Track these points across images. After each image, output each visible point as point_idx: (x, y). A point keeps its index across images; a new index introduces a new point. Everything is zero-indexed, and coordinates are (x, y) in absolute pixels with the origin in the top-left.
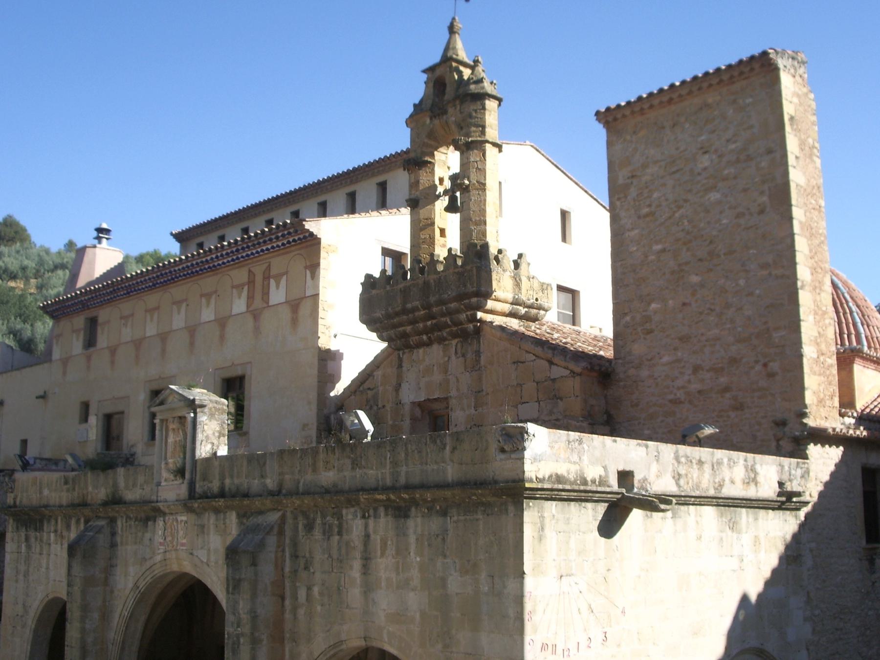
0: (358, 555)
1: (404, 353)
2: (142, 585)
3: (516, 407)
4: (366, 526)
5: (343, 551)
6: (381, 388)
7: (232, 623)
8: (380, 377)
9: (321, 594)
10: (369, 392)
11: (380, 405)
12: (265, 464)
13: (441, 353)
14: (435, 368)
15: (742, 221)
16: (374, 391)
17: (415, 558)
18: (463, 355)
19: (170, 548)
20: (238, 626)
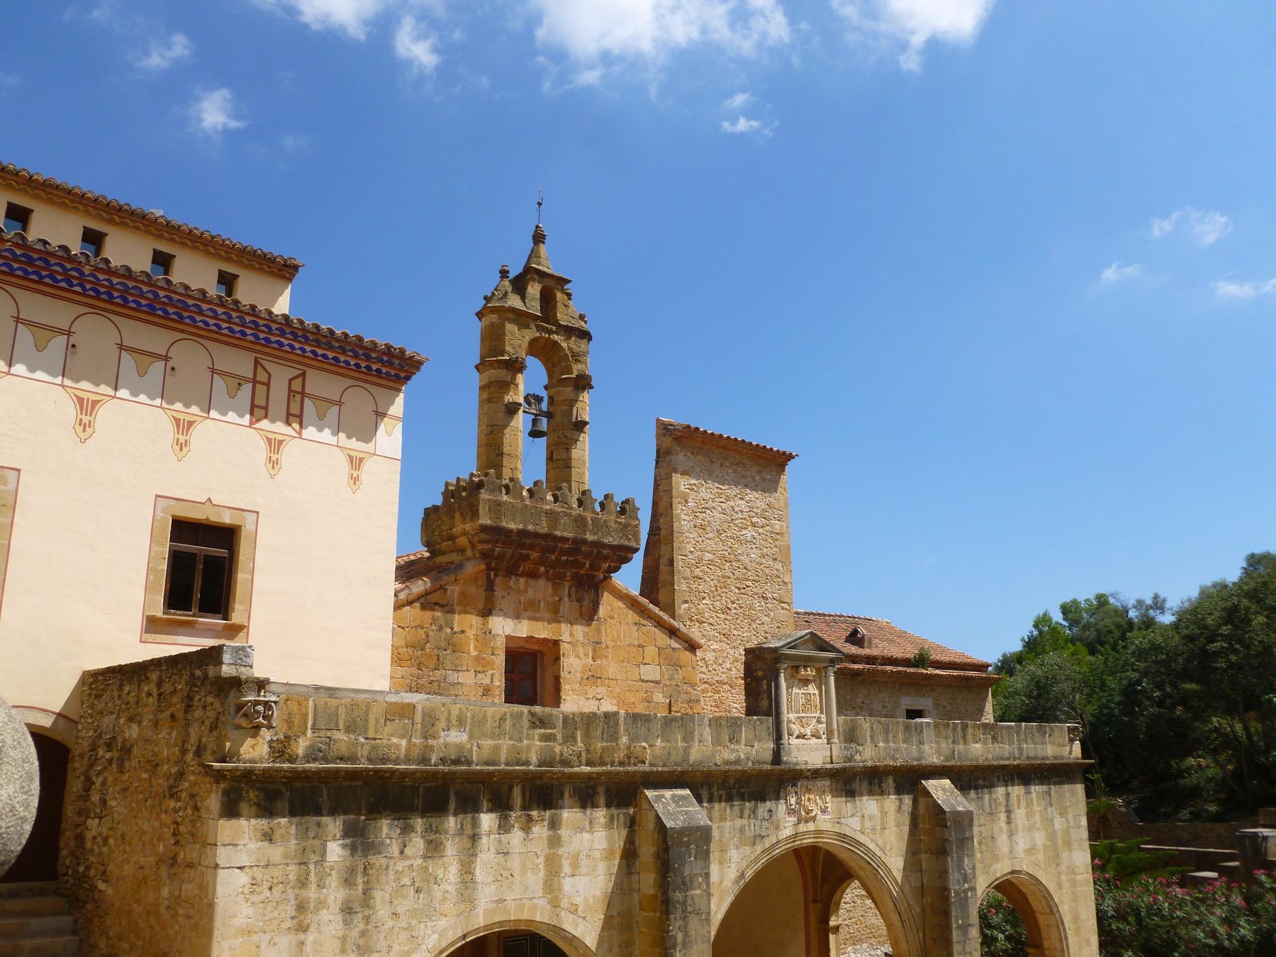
1: (496, 575)
2: (749, 874)
3: (638, 666)
5: (993, 807)
7: (958, 881)
8: (456, 594)
12: (922, 731)
13: (550, 591)
14: (542, 604)
15: (763, 560)
17: (1036, 808)
18: (579, 601)
20: (965, 881)
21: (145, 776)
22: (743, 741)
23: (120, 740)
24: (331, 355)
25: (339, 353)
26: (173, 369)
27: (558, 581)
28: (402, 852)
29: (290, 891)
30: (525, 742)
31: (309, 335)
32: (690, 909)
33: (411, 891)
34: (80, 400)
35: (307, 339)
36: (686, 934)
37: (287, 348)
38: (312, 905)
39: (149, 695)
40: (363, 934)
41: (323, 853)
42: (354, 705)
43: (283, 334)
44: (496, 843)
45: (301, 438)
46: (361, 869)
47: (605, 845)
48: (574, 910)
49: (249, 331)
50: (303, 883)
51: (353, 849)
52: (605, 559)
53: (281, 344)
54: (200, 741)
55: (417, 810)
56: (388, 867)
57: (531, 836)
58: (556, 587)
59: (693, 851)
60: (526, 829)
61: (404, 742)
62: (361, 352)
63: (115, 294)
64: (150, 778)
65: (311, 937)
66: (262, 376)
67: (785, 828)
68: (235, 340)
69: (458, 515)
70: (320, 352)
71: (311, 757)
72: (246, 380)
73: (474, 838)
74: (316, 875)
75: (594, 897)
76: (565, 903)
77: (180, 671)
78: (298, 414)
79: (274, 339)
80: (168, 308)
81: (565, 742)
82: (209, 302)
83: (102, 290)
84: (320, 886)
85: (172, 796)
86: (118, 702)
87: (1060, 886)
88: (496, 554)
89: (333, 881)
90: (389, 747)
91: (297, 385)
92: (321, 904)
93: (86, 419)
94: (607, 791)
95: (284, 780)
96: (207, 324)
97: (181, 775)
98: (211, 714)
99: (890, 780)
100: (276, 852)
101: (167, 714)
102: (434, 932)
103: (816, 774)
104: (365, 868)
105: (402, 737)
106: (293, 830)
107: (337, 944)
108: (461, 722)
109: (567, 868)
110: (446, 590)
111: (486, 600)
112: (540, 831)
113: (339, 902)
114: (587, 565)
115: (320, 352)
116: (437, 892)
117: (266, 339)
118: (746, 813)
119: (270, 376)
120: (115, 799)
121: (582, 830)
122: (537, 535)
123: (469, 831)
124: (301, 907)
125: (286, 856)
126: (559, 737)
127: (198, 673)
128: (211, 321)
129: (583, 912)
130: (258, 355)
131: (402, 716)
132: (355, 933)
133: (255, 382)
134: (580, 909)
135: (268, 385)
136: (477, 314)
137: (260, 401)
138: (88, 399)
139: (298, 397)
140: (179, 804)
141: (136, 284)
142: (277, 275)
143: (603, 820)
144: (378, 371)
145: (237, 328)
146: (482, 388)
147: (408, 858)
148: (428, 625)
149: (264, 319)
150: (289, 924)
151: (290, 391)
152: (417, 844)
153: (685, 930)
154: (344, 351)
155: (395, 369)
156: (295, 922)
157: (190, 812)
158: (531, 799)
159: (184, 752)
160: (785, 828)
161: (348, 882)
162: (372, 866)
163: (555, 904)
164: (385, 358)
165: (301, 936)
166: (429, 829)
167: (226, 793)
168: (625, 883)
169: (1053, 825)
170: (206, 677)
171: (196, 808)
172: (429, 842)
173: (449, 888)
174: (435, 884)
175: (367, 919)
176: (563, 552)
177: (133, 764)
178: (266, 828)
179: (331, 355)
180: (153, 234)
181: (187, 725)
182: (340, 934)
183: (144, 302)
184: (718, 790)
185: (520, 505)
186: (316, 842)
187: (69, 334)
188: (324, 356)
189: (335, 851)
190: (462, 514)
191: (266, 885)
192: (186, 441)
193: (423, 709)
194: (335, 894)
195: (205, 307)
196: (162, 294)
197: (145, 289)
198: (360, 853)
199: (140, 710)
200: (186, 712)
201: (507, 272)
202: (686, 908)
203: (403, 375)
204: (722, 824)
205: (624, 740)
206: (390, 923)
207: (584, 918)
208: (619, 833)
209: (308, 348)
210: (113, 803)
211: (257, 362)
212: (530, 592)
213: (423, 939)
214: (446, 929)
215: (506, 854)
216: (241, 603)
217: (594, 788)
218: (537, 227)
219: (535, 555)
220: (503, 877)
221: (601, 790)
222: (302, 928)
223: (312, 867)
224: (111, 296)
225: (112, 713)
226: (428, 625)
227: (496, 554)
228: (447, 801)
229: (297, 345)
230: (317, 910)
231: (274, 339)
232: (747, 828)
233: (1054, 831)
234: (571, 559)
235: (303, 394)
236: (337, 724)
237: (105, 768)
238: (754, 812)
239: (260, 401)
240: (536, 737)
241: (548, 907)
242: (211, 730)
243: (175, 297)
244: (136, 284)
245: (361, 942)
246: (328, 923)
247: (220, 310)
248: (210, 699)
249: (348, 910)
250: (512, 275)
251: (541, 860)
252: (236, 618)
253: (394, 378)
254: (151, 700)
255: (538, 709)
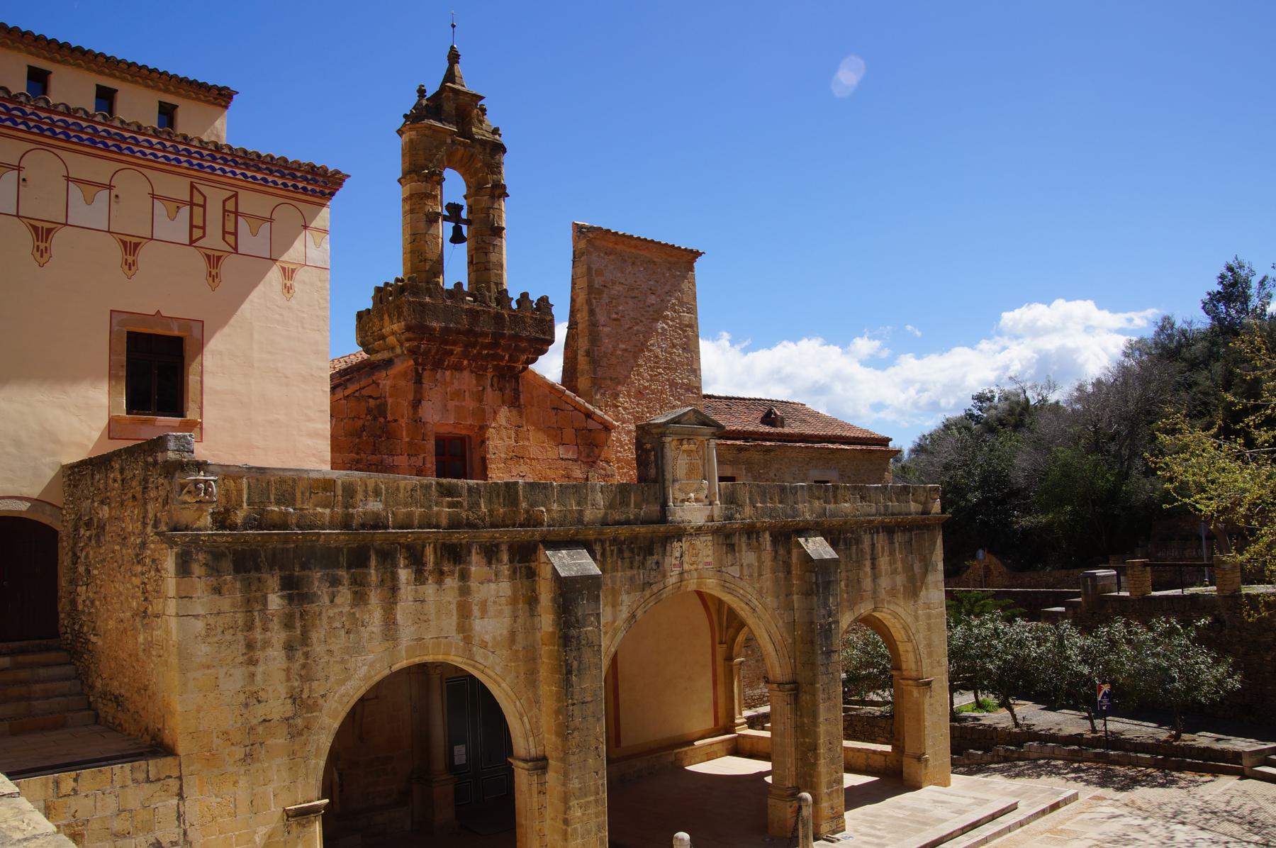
0: (868, 557)
1: (424, 370)
4: (872, 539)
5: (860, 556)
6: (390, 401)
7: (824, 616)
8: (388, 388)
9: (847, 586)
10: (370, 400)
11: (390, 418)
12: (796, 493)
13: (474, 382)
14: (467, 394)
16: (379, 401)
17: (898, 556)
18: (500, 390)
19: (686, 567)
20: (829, 617)
21: (117, 547)
22: (632, 505)
23: (95, 520)
24: (259, 176)
25: (266, 174)
26: (117, 196)
27: (481, 373)
28: (332, 601)
29: (239, 634)
30: (435, 509)
31: (237, 159)
32: (583, 642)
33: (343, 632)
34: (35, 229)
35: (236, 163)
36: (580, 663)
37: (219, 172)
38: (259, 645)
39: (115, 481)
40: (304, 666)
41: (265, 604)
42: (283, 481)
43: (214, 159)
44: (413, 593)
45: (237, 253)
46: (298, 615)
47: (509, 593)
48: (484, 645)
49: (183, 159)
50: (249, 627)
51: (290, 599)
52: (524, 351)
53: (213, 169)
54: (156, 515)
55: (343, 567)
56: (320, 613)
57: (444, 587)
58: (480, 378)
59: (586, 596)
60: (440, 582)
61: (328, 511)
62: (286, 172)
63: (58, 131)
64: (121, 549)
65: (260, 670)
66: (198, 199)
67: (671, 576)
68: (172, 165)
69: (386, 317)
70: (249, 174)
71: (248, 524)
72: (183, 202)
73: (394, 589)
74: (261, 620)
75: (501, 635)
76: (476, 641)
77: (136, 459)
78: (233, 231)
79: (206, 164)
80: (107, 141)
81: (470, 508)
82: (144, 134)
83: (45, 127)
84: (265, 629)
85: (139, 562)
86: (92, 489)
87: (917, 618)
88: (422, 350)
89: (275, 625)
90: (315, 515)
91: (230, 206)
92: (266, 644)
93: (42, 246)
94: (511, 548)
95: (227, 545)
96: (144, 154)
97: (144, 545)
98: (163, 493)
99: (767, 535)
100: (225, 603)
101: (130, 495)
102: (364, 665)
103: (699, 531)
104: (302, 615)
105: (325, 507)
106: (238, 585)
107: (283, 674)
108: (377, 493)
109: (476, 611)
110: (378, 385)
111: (415, 392)
112: (451, 583)
113: (282, 642)
114: (507, 358)
115: (249, 174)
116: (365, 633)
117: (200, 165)
118: (636, 564)
119: (205, 198)
120: (96, 568)
121: (490, 581)
122: (458, 332)
123: (389, 584)
124: (250, 646)
125: (233, 605)
126: (465, 504)
127: (150, 459)
128: (148, 151)
129: (492, 647)
130: (193, 180)
131: (325, 489)
132: (297, 666)
133: (192, 204)
134: (490, 644)
135: (204, 206)
136: (398, 132)
137: (198, 221)
138: (42, 228)
139: (233, 216)
140: (144, 568)
141: (75, 121)
142: (213, 104)
143: (507, 573)
144: (304, 189)
145: (172, 157)
146: (404, 200)
147: (336, 606)
148: (364, 416)
149: (195, 146)
150: (241, 659)
151: (225, 211)
152: (345, 595)
153: (579, 659)
154: (271, 173)
155: (319, 186)
156: (246, 657)
157: (153, 573)
158: (442, 555)
159: (145, 525)
160: (671, 576)
161: (288, 624)
162: (307, 612)
163: (468, 640)
164: (309, 177)
165: (252, 668)
166: (353, 582)
167: (178, 556)
168: (528, 623)
169: (913, 569)
170: (156, 463)
171: (158, 570)
172: (355, 593)
173: (375, 630)
174: (363, 626)
175: (306, 655)
176: (484, 347)
177: (107, 539)
178: (215, 583)
179: (259, 176)
180: (95, 71)
181: (146, 503)
182: (285, 666)
183: (85, 137)
184: (610, 546)
185: (442, 306)
186: (259, 594)
187: (19, 168)
188: (254, 178)
189: (275, 602)
190: (389, 316)
191: (220, 630)
192: (134, 261)
193: (343, 483)
194: (278, 636)
195: (140, 138)
196: (100, 128)
197: (84, 124)
198: (296, 602)
199: (109, 494)
200: (144, 493)
201: (425, 91)
202: (580, 642)
203: (327, 191)
204: (614, 574)
205: (524, 505)
206: (326, 658)
207: (493, 653)
208: (522, 583)
209: (238, 171)
210: (95, 572)
211: (192, 187)
212: (456, 383)
213: (355, 670)
214: (374, 662)
215: (423, 601)
216: (194, 402)
217: (497, 546)
218: (452, 47)
219: (458, 349)
220: (420, 619)
221: (504, 547)
222: (253, 662)
223: (256, 614)
224: (54, 133)
225: (87, 499)
226: (364, 416)
227: (422, 350)
228: (368, 559)
229: (227, 169)
230: (263, 648)
231: (206, 164)
232: (637, 577)
233: (914, 575)
234: (491, 352)
235: (236, 213)
236: (269, 498)
237: (87, 544)
238: (643, 564)
239: (198, 221)
240: (445, 504)
241: (462, 644)
242: (164, 506)
243: (113, 131)
244: (75, 121)
245: (303, 672)
246: (273, 659)
247: (154, 141)
248: (161, 480)
249: (289, 648)
250: (429, 94)
251: (454, 607)
252: (191, 415)
253: (319, 194)
254: (116, 485)
255: (444, 481)
